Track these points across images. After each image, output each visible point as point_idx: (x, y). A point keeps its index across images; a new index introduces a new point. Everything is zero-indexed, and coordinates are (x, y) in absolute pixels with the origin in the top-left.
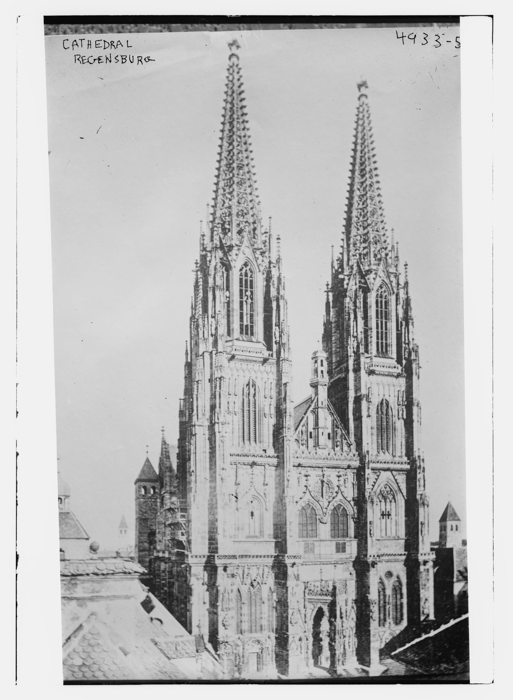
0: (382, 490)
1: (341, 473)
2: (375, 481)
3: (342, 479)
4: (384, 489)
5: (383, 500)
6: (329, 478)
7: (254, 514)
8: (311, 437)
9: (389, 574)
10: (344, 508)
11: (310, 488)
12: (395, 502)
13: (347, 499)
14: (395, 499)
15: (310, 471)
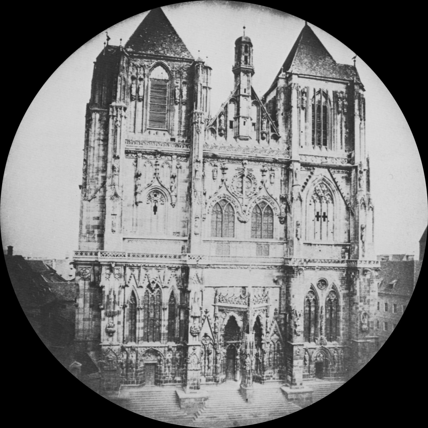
0: (317, 189)
1: (266, 168)
2: (308, 178)
3: (267, 174)
4: (320, 188)
5: (318, 201)
6: (251, 172)
7: (158, 209)
8: (231, 127)
9: (323, 282)
10: (268, 206)
11: (227, 183)
12: (333, 203)
13: (273, 196)
14: (332, 199)
15: (228, 165)
